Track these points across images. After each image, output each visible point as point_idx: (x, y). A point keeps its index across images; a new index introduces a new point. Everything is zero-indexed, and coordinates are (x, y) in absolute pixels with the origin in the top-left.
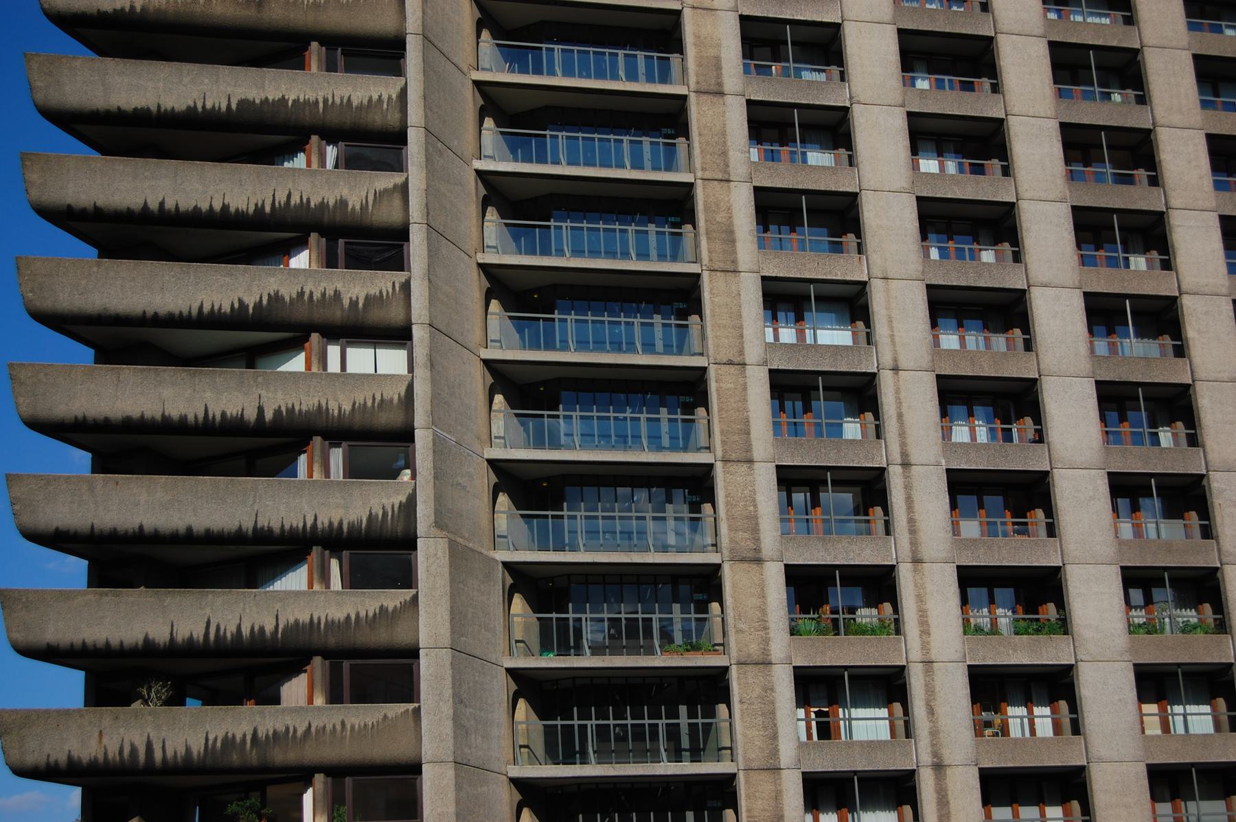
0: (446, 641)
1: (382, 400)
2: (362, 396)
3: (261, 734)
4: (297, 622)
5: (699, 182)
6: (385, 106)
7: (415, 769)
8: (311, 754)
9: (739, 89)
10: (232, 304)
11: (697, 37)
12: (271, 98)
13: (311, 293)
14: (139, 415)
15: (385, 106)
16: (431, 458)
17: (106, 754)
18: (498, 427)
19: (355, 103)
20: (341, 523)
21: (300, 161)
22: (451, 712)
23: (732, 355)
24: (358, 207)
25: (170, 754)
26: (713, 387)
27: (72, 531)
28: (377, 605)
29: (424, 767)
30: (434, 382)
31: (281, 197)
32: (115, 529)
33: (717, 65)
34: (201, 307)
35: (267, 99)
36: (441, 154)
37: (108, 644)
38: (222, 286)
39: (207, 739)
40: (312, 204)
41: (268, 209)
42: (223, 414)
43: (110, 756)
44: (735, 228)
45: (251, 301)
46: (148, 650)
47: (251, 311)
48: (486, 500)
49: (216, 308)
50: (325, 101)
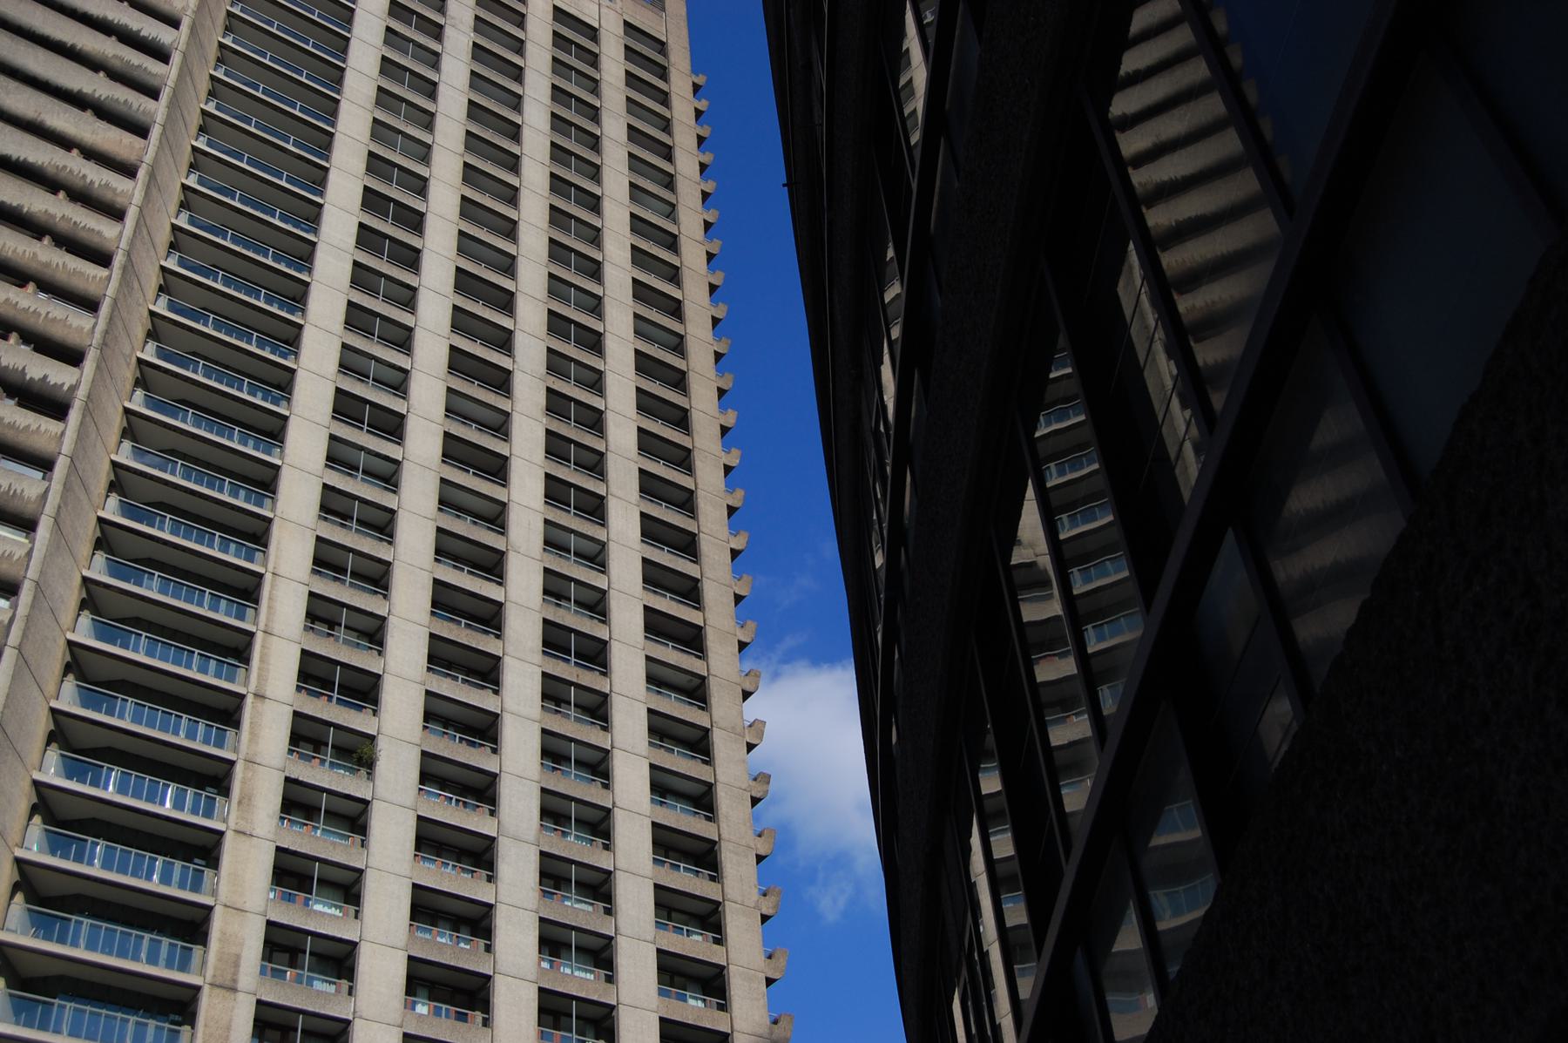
9: (252, 988)
33: (236, 963)
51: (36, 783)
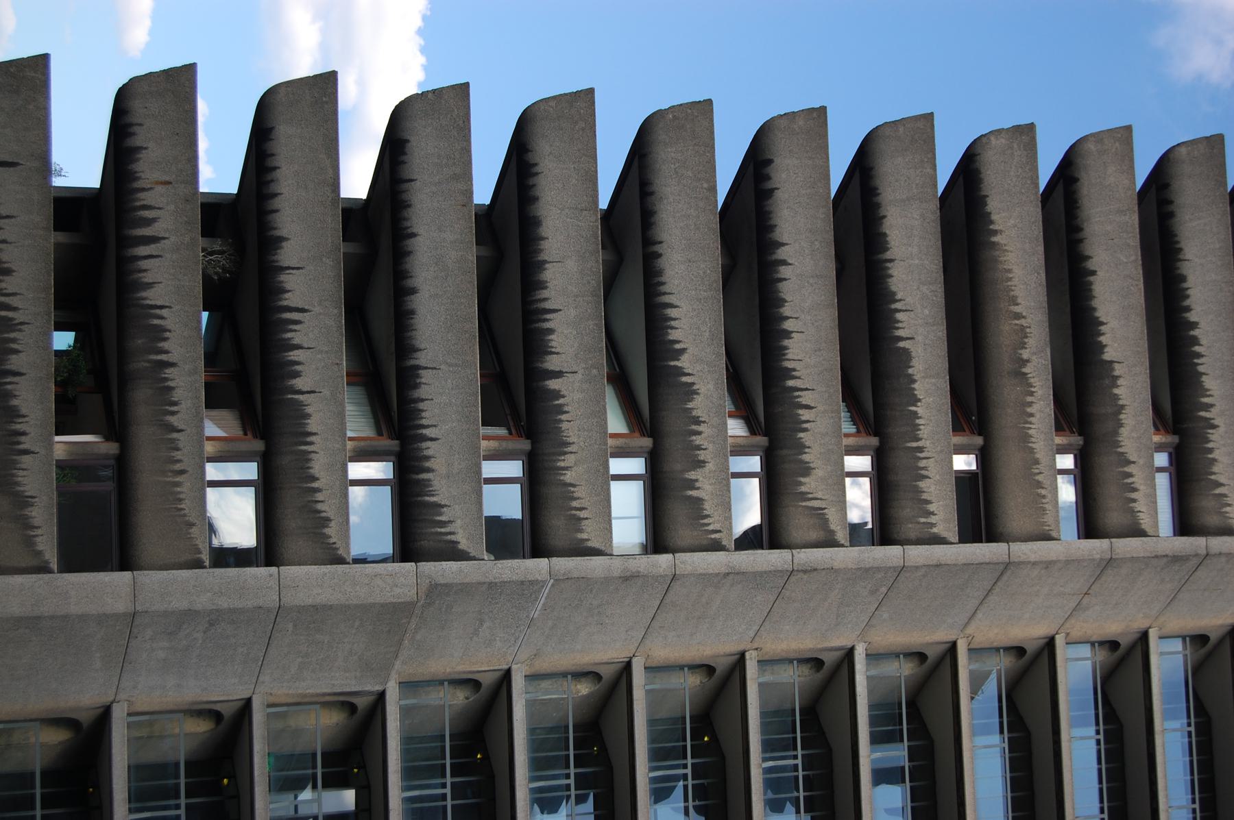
0: (290, 599)
3: (169, 373)
4: (308, 416)
6: (923, 520)
7: (125, 564)
8: (144, 435)
12: (916, 386)
13: (700, 433)
15: (923, 520)
17: (144, 190)
18: (551, 692)
19: (922, 484)
20: (429, 470)
22: (198, 607)
24: (803, 489)
25: (144, 264)
27: (404, 158)
28: (330, 514)
29: (127, 575)
30: (607, 581)
31: (806, 398)
32: (409, 206)
35: (914, 381)
36: (873, 592)
37: (276, 195)
38: (698, 328)
39: (162, 307)
40: (801, 435)
41: (791, 383)
42: (551, 331)
43: (141, 195)
45: (684, 362)
46: (268, 242)
47: (672, 363)
48: (460, 668)
49: (673, 323)
50: (921, 449)
51: (1144, 637)
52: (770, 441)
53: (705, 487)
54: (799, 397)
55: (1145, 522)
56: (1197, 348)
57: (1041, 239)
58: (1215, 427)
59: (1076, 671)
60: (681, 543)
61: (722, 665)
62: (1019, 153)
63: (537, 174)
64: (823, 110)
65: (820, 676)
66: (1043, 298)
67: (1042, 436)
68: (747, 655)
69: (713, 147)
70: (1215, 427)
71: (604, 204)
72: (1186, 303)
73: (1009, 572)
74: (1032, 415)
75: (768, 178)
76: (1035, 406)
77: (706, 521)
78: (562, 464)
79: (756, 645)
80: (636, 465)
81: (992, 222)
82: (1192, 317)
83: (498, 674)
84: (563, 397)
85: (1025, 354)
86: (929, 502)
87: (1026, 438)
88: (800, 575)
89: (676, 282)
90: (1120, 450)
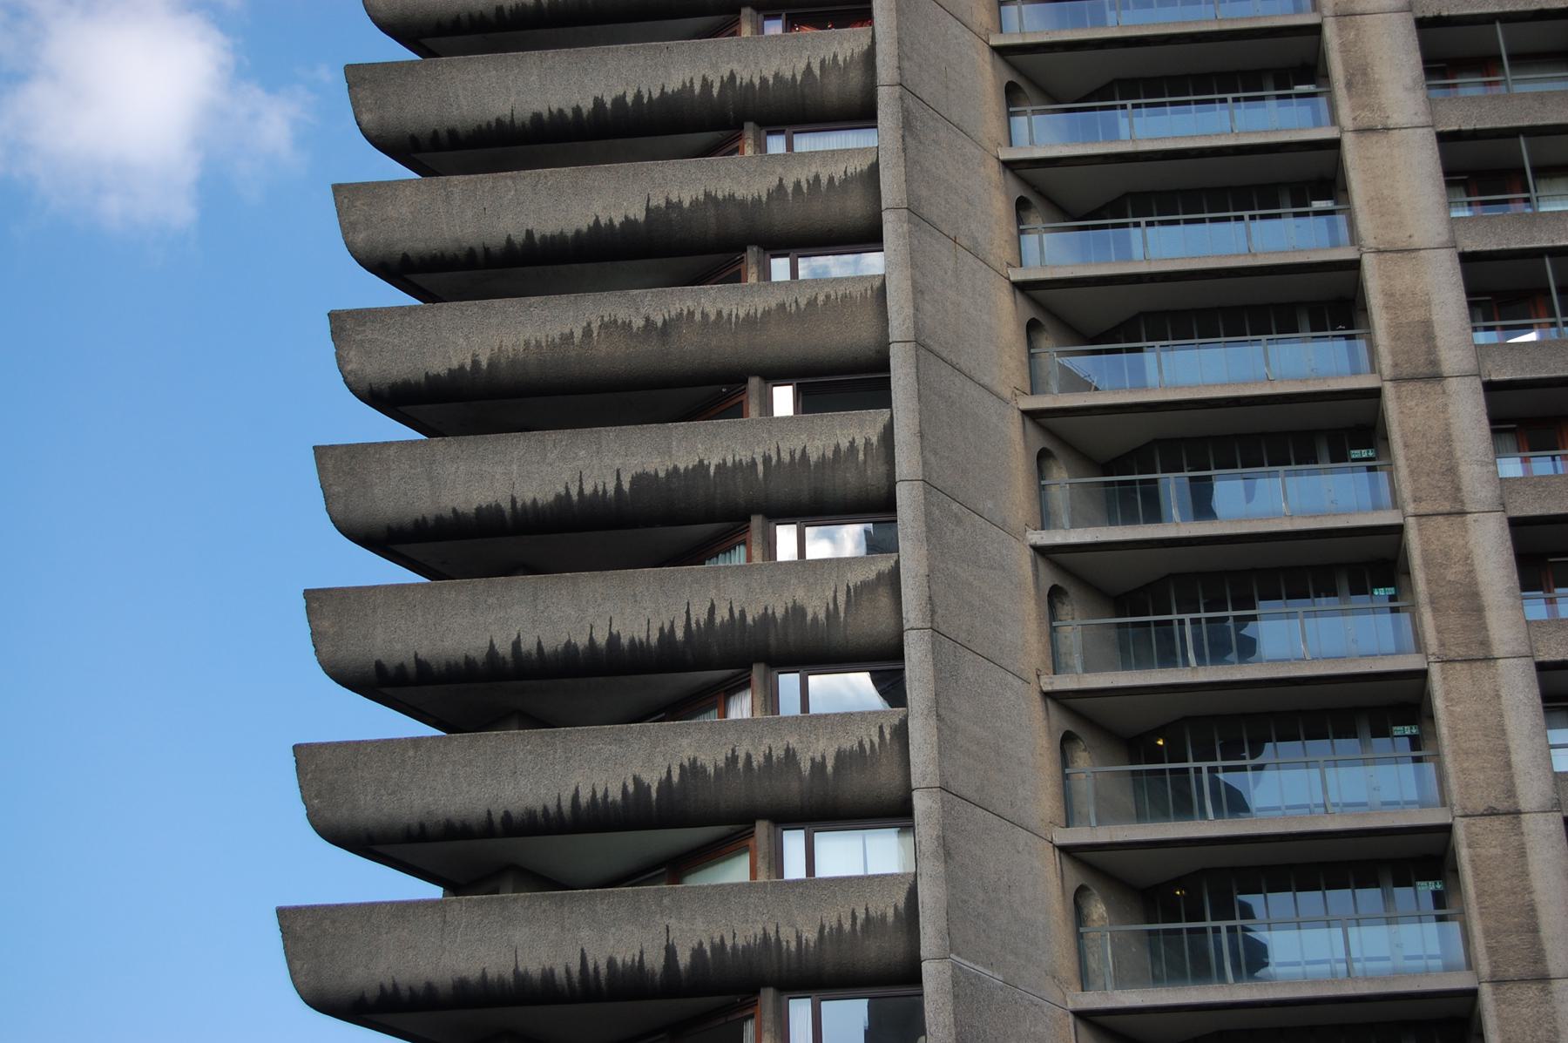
1: (868, 918)
2: (834, 915)
5: (1411, 520)
6: (861, 456)
10: (625, 787)
11: (1389, 294)
12: (682, 467)
13: (749, 757)
14: (478, 974)
15: (861, 456)
16: (950, 1008)
18: (1103, 955)
19: (814, 457)
21: (739, 557)
23: (1494, 798)
24: (822, 616)
26: (1464, 855)
30: (950, 880)
31: (700, 614)
33: (1427, 332)
34: (576, 797)
35: (676, 468)
36: (959, 522)
40: (749, 619)
41: (680, 634)
42: (611, 962)
44: (1482, 588)
45: (653, 779)
49: (599, 795)
50: (767, 460)
51: (1009, 166)
52: (758, 661)
53: (821, 748)
54: (698, 623)
55: (859, 165)
56: (629, 99)
57: (485, 302)
58: (732, 76)
59: (1057, 253)
60: (898, 780)
61: (1061, 723)
62: (368, 332)
63: (395, 986)
64: (309, 595)
65: (1072, 590)
66: (563, 299)
67: (747, 299)
68: (1047, 688)
69: (359, 743)
70: (732, 76)
71: (435, 892)
72: (569, 112)
73: (928, 341)
74: (719, 313)
75: (401, 668)
76: (707, 310)
77: (867, 747)
78: (793, 945)
79: (1033, 677)
80: (793, 842)
81: (462, 368)
82: (587, 105)
83: (1082, 1029)
84: (701, 944)
85: (639, 322)
86: (837, 446)
87: (750, 321)
88: (938, 619)
89: (543, 791)
90: (764, 199)
